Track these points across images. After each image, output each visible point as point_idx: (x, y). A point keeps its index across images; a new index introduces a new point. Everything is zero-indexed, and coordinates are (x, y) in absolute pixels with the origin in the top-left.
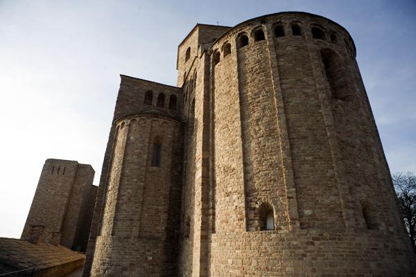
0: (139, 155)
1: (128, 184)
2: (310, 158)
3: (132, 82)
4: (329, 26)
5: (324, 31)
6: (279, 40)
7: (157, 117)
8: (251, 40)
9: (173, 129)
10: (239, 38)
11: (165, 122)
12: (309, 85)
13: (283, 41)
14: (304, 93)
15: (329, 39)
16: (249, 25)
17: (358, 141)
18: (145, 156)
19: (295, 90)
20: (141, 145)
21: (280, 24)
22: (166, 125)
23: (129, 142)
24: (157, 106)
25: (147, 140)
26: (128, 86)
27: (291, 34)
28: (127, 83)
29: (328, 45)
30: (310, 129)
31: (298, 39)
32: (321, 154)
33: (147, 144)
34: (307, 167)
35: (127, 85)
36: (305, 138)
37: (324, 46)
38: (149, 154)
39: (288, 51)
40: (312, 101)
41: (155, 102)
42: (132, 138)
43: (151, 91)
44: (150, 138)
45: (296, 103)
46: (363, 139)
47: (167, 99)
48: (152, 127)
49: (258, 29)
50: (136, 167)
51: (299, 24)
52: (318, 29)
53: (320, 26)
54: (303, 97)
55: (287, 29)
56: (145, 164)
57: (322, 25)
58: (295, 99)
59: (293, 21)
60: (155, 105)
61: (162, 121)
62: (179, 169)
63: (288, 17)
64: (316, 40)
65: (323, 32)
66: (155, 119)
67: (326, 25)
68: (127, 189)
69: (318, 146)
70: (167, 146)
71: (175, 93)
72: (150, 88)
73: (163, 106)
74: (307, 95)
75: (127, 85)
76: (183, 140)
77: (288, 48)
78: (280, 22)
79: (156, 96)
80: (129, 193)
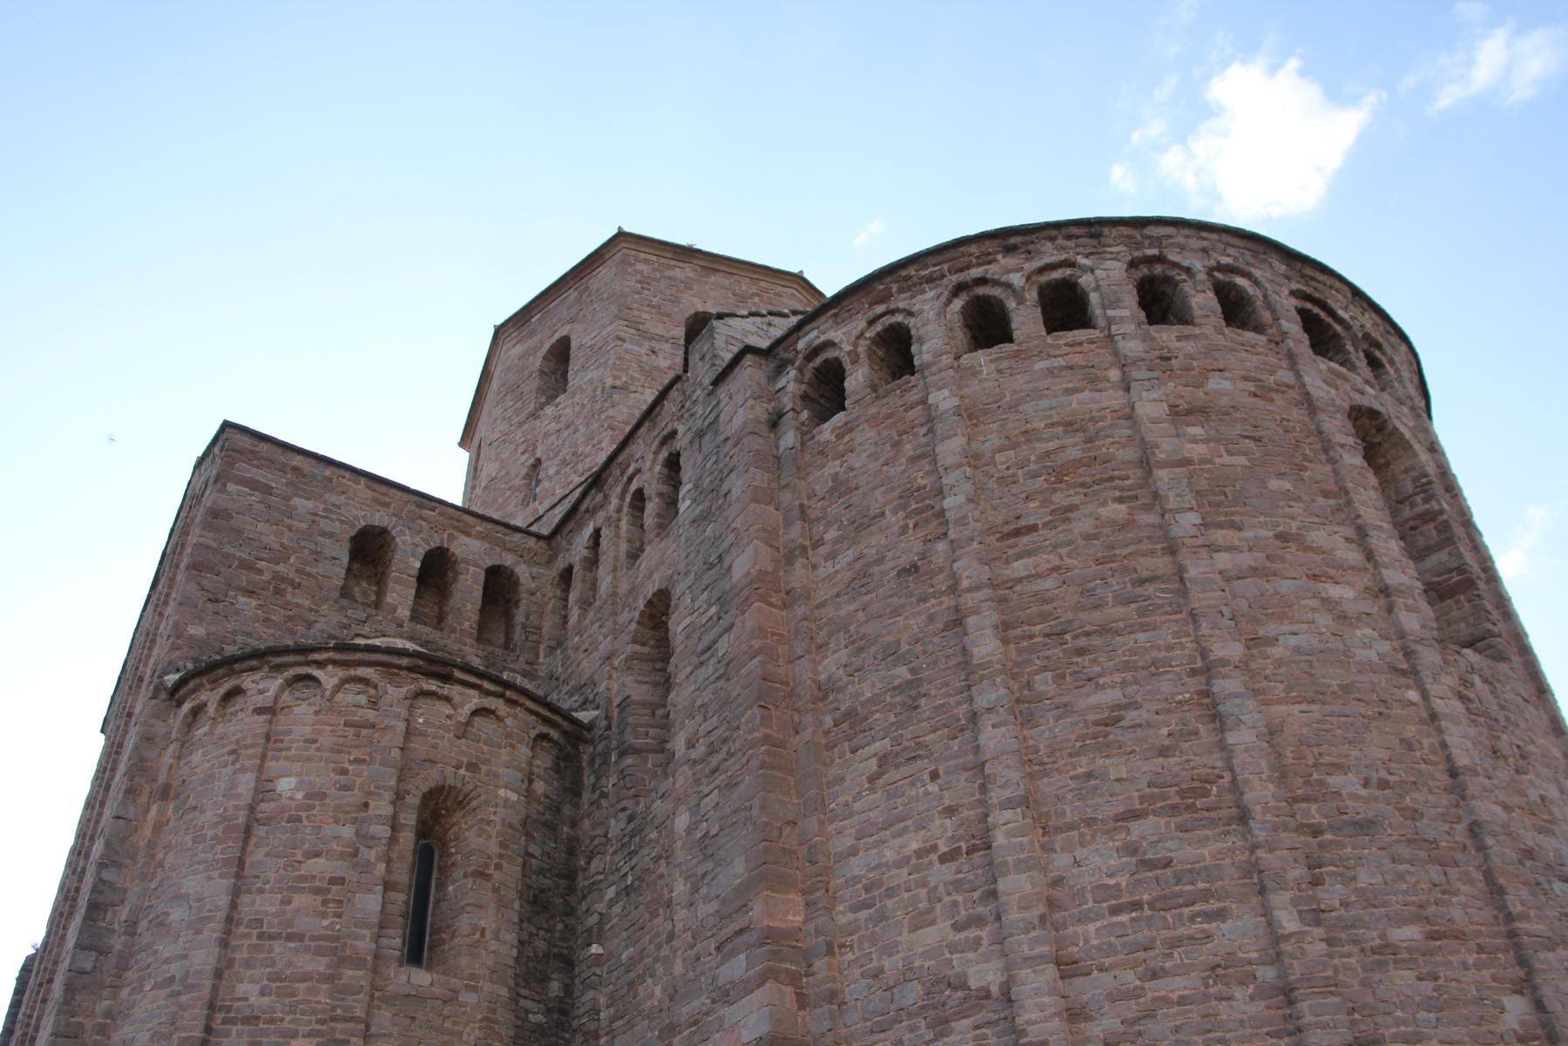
0: (331, 892)
3: (283, 469)
6: (1167, 335)
7: (446, 678)
8: (1026, 319)
9: (524, 751)
10: (958, 304)
11: (477, 712)
13: (1189, 347)
15: (1366, 371)
16: (1010, 250)
18: (370, 903)
20: (348, 832)
21: (1158, 269)
22: (484, 726)
23: (266, 807)
24: (415, 616)
25: (383, 807)
26: (267, 490)
28: (253, 473)
29: (1371, 397)
30: (1383, 785)
31: (1251, 348)
33: (383, 831)
34: (1402, 979)
35: (253, 485)
36: (1365, 827)
37: (1359, 400)
38: (388, 886)
39: (1221, 394)
41: (401, 594)
42: (285, 785)
43: (383, 531)
44: (399, 797)
45: (1297, 650)
47: (468, 589)
48: (409, 733)
49: (1057, 275)
50: (320, 965)
54: (1324, 620)
55: (1202, 301)
56: (365, 945)
58: (1286, 628)
59: (1220, 268)
60: (404, 612)
61: (474, 700)
62: (555, 987)
63: (1194, 243)
64: (1323, 364)
65: (1336, 335)
66: (432, 685)
67: (1346, 309)
69: (1435, 872)
70: (493, 847)
71: (508, 560)
72: (380, 518)
73: (439, 621)
75: (253, 485)
76: (574, 824)
77: (1216, 383)
78: (1160, 259)
79: (408, 556)
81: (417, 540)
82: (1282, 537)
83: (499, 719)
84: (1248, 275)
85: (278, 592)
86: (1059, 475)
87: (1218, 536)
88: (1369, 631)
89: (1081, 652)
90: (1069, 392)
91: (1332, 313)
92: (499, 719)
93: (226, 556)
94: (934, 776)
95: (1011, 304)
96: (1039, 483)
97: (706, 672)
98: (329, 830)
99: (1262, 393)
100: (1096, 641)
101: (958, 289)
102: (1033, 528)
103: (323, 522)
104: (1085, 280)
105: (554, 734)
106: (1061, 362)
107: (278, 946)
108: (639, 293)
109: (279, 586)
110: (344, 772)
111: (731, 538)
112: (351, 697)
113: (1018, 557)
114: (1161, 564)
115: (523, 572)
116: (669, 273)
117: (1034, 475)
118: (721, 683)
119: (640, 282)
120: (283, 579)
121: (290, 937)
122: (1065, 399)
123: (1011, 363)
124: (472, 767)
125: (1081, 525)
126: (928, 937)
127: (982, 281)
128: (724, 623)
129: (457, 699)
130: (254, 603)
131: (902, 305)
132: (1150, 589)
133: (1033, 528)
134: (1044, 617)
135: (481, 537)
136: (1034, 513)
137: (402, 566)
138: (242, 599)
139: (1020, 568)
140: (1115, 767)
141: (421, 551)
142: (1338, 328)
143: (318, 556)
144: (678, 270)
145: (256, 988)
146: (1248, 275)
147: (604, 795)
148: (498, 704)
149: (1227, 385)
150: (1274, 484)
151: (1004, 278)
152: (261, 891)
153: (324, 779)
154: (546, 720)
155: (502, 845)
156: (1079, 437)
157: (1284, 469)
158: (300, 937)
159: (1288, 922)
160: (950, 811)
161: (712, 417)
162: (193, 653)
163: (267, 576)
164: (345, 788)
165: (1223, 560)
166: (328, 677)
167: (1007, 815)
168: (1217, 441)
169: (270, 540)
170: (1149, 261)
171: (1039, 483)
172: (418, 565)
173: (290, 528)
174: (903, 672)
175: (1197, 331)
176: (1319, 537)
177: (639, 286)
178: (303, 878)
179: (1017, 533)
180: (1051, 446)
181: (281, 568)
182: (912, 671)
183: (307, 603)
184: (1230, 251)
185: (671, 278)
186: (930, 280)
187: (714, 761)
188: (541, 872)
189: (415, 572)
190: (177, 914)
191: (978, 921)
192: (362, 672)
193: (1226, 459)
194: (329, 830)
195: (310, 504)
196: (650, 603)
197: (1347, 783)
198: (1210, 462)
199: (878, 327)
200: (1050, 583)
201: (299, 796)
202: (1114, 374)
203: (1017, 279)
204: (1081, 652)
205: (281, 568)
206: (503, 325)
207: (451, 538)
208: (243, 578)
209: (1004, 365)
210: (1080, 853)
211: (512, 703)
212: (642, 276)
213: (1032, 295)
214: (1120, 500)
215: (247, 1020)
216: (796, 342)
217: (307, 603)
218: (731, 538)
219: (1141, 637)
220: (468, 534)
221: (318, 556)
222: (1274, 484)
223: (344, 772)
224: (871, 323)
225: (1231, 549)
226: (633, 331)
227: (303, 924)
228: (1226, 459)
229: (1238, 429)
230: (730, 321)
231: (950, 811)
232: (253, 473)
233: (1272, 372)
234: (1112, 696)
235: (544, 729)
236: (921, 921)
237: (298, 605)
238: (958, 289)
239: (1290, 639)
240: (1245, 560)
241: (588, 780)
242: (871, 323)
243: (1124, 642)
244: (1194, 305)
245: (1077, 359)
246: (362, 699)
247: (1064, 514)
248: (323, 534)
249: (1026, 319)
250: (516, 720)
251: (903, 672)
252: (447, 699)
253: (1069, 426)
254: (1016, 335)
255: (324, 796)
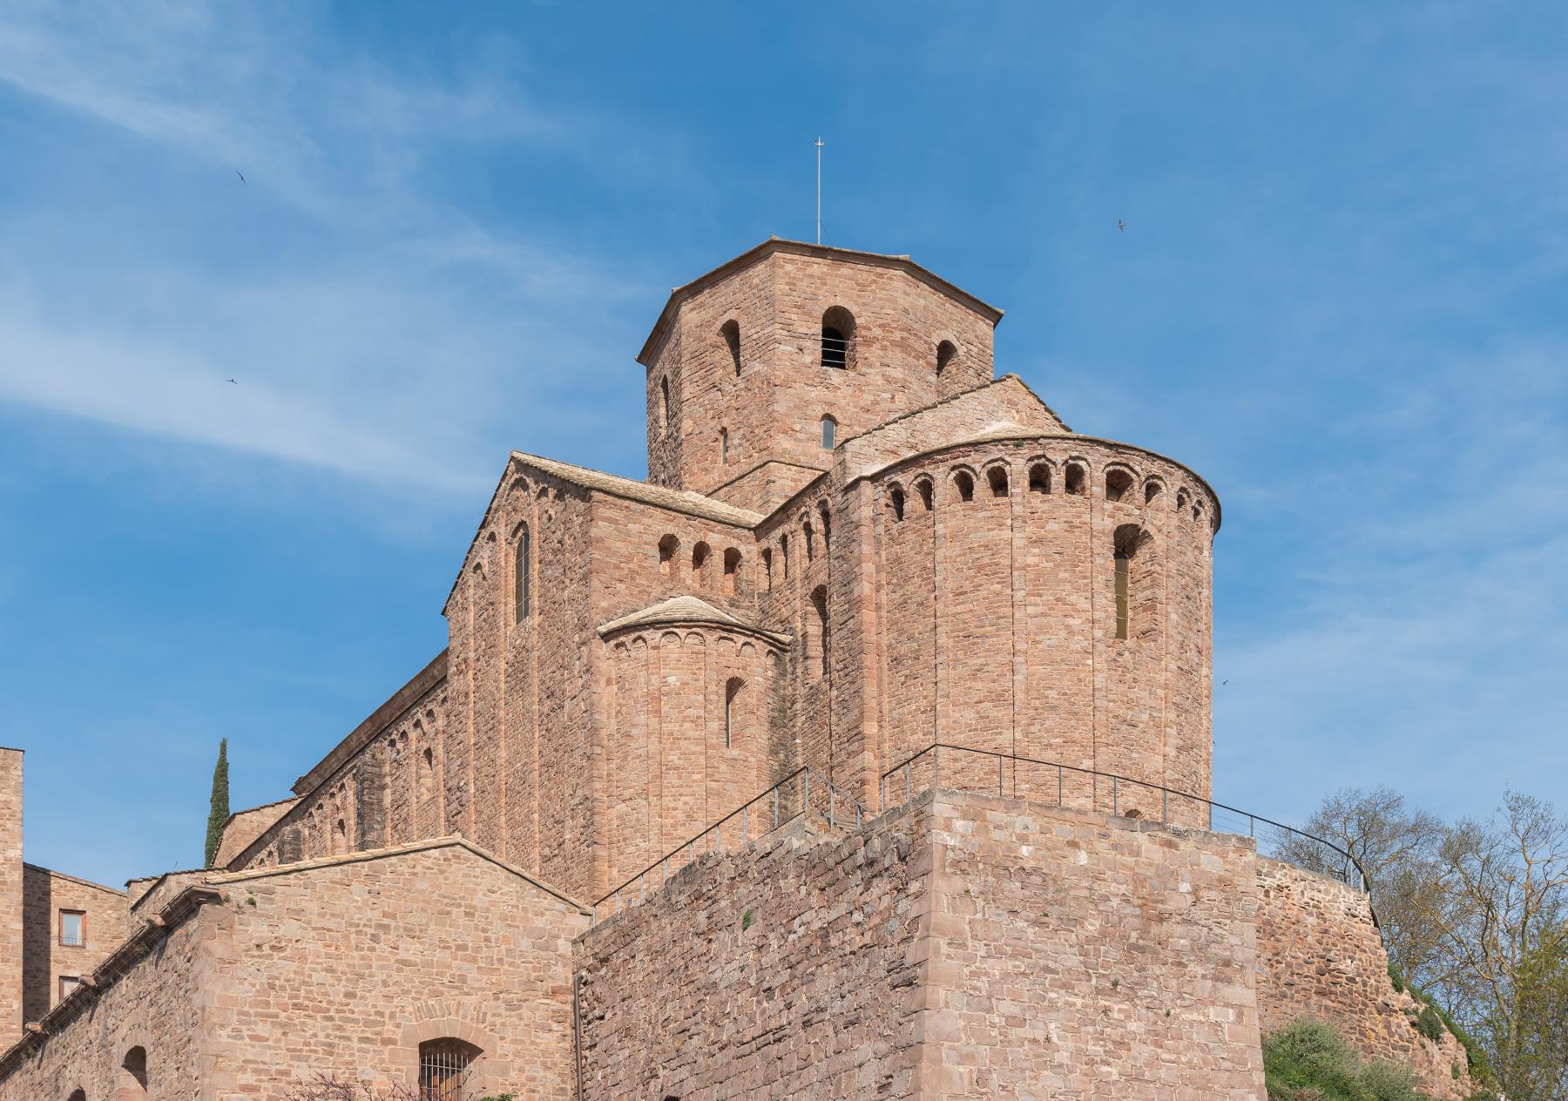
1: (681, 786)
2: (1060, 740)
4: (1147, 464)
5: (1133, 475)
10: (953, 474)
11: (744, 644)
12: (1078, 611)
13: (1046, 506)
14: (1067, 627)
17: (1145, 717)
19: (1052, 620)
22: (747, 649)
27: (1062, 489)
28: (608, 513)
32: (1076, 735)
36: (1053, 708)
39: (1051, 531)
40: (1079, 643)
42: (671, 679)
43: (672, 536)
45: (1049, 646)
46: (1155, 714)
50: (693, 748)
51: (1082, 463)
52: (1123, 472)
53: (1127, 465)
54: (1063, 634)
55: (1058, 478)
57: (1131, 464)
58: (1048, 636)
59: (1071, 458)
61: (743, 639)
64: (1109, 506)
68: (681, 795)
70: (755, 701)
71: (734, 543)
74: (1071, 632)
77: (1051, 526)
78: (1044, 456)
80: (685, 803)
81: (689, 539)
82: (1057, 600)
83: (753, 646)
84: (1085, 460)
85: (633, 579)
86: (980, 569)
87: (1032, 599)
88: (1080, 637)
89: (974, 644)
90: (990, 530)
91: (1132, 469)
92: (753, 646)
93: (607, 562)
94: (922, 684)
95: (975, 479)
96: (972, 572)
97: (844, 633)
98: (693, 697)
99: (1072, 527)
100: (980, 640)
101: (954, 468)
102: (966, 593)
103: (644, 536)
104: (1007, 469)
105: (774, 649)
106: (989, 514)
107: (682, 742)
108: (788, 295)
109: (633, 574)
110: (695, 674)
111: (853, 576)
112: (692, 640)
113: (959, 604)
114: (1007, 611)
115: (742, 549)
116: (809, 271)
117: (969, 569)
118: (850, 640)
119: (788, 284)
120: (633, 571)
121: (686, 739)
122: (987, 533)
123: (970, 512)
124: (744, 668)
125: (983, 593)
126: (916, 737)
127: (964, 466)
128: (850, 614)
129: (735, 639)
130: (624, 586)
131: (930, 472)
132: (1002, 621)
133: (966, 593)
134: (964, 629)
135: (720, 532)
136: (968, 586)
137: (684, 556)
138: (619, 585)
139: (959, 608)
140: (979, 685)
141: (692, 546)
142: (1133, 475)
143: (646, 557)
144: (816, 266)
145: (676, 758)
146: (1085, 460)
147: (797, 677)
148: (752, 640)
149: (1056, 527)
150: (1062, 575)
151: (973, 466)
152: (670, 722)
153: (688, 677)
154: (770, 644)
155: (759, 700)
156: (990, 552)
157: (1068, 568)
158: (689, 739)
159: (1018, 736)
160: (925, 697)
161: (844, 505)
162: (605, 615)
163: (626, 572)
164: (696, 680)
165: (1030, 610)
166: (682, 632)
167: (942, 700)
168: (1043, 555)
169: (623, 551)
170: (1039, 457)
171: (972, 572)
172: (692, 554)
173: (630, 542)
174: (915, 645)
175: (1050, 497)
176: (1073, 599)
177: (788, 288)
178: (685, 717)
179: (960, 594)
180: (977, 556)
181: (631, 565)
182: (919, 645)
183: (645, 583)
184: (1079, 448)
185: (811, 276)
186: (942, 461)
187: (847, 671)
188: (773, 710)
189: (691, 558)
190: (634, 732)
191: (931, 733)
192: (694, 630)
193: (1046, 564)
194: (693, 697)
195: (637, 526)
196: (816, 589)
197: (1052, 694)
198: (1038, 566)
199: (919, 480)
200: (967, 616)
201: (678, 684)
202: (1009, 522)
203: (977, 467)
204: (974, 644)
205: (631, 565)
206: (679, 292)
207: (706, 535)
208: (617, 574)
209: (967, 512)
210: (963, 713)
211: (757, 638)
212: (790, 278)
213: (984, 475)
214: (998, 583)
215: (674, 769)
216: (883, 477)
217: (645, 583)
218: (853, 576)
219: (995, 639)
220: (713, 532)
221: (646, 557)
222: (1062, 575)
223: (695, 674)
224: (916, 478)
225: (1035, 605)
226: (785, 333)
227: (690, 733)
228: (1046, 564)
229: (1055, 549)
230: (853, 442)
231: (925, 697)
232: (608, 513)
233: (1079, 517)
234: (982, 661)
235: (771, 648)
236: (914, 732)
237: (643, 585)
238: (954, 468)
239: (1048, 641)
240: (1041, 609)
241: (790, 669)
242: (916, 478)
243: (990, 641)
244: (1053, 482)
245: (996, 513)
246: (697, 641)
247: (977, 588)
248: (646, 543)
249: (981, 487)
250: (761, 646)
251: (915, 645)
252: (732, 640)
253: (986, 547)
254: (974, 497)
255: (688, 684)
